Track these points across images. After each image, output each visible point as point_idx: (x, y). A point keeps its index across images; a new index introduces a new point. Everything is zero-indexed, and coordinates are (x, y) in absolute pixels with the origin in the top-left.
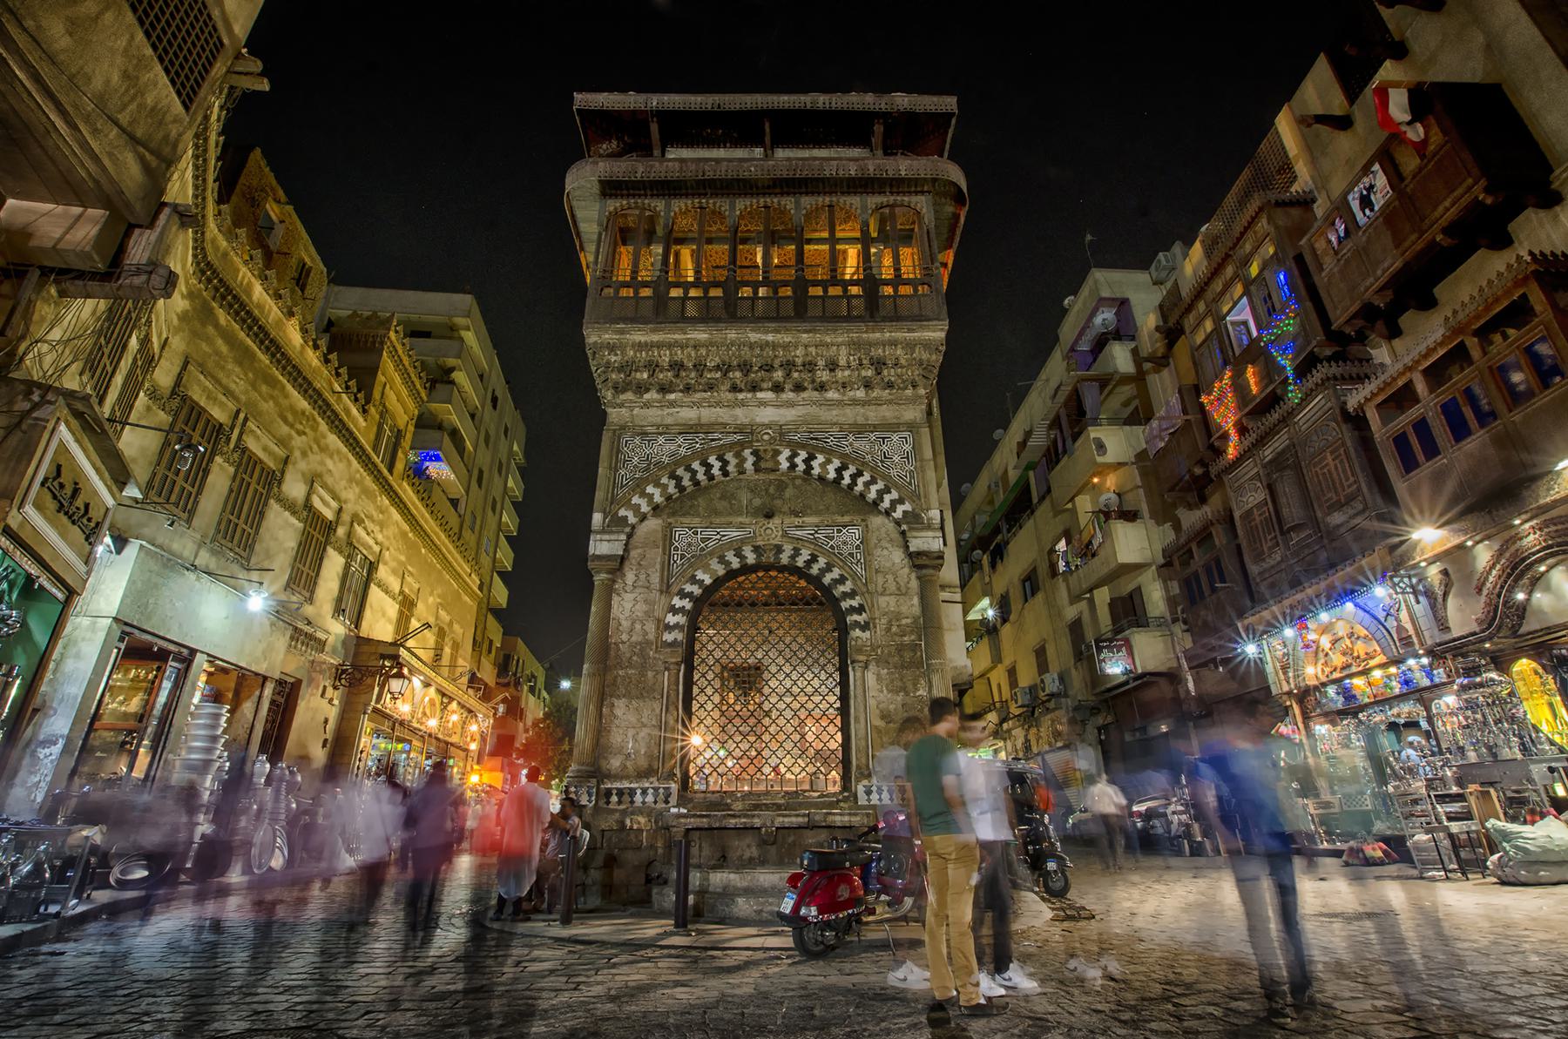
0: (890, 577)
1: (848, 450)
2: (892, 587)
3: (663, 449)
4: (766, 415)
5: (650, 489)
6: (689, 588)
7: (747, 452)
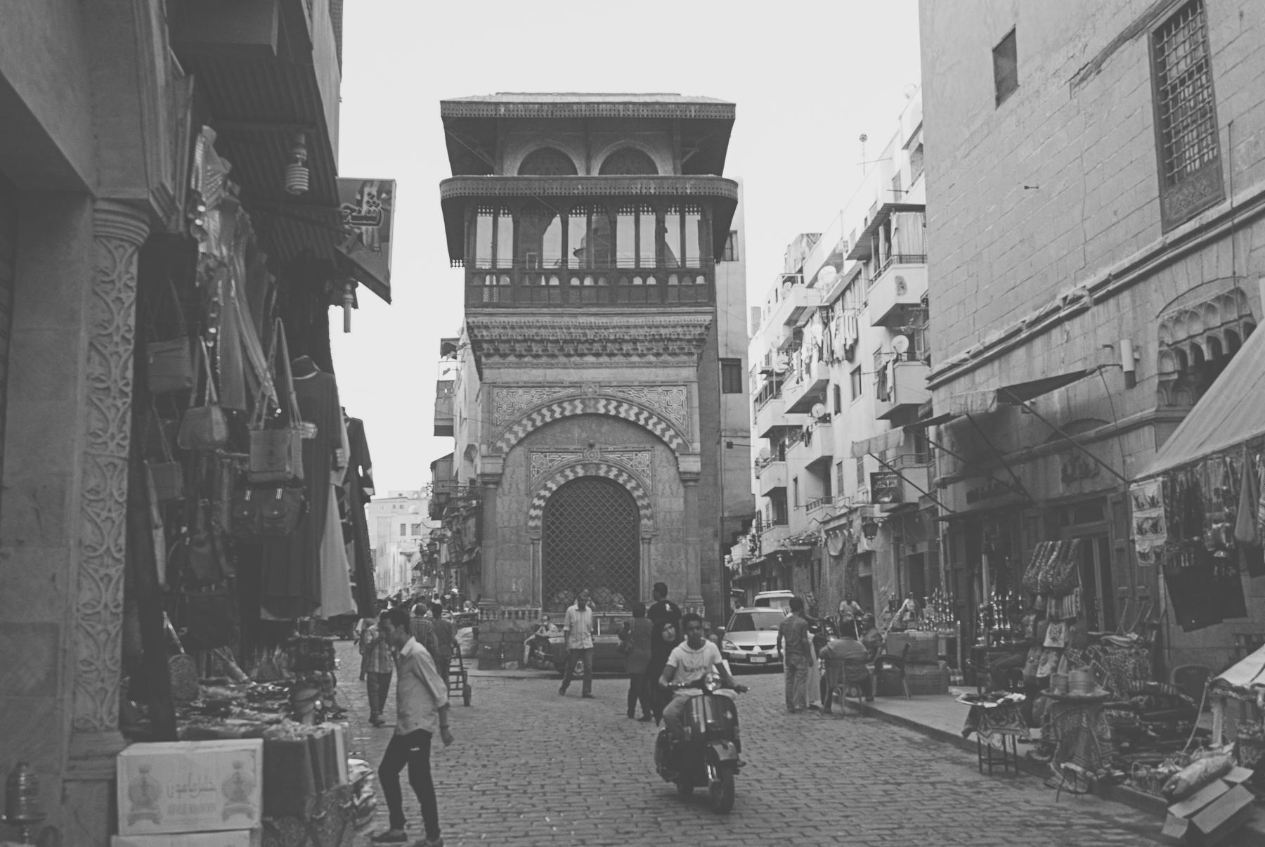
0: (667, 486)
1: (643, 400)
2: (668, 491)
3: (523, 399)
4: (589, 375)
5: (516, 428)
6: (543, 493)
7: (577, 402)
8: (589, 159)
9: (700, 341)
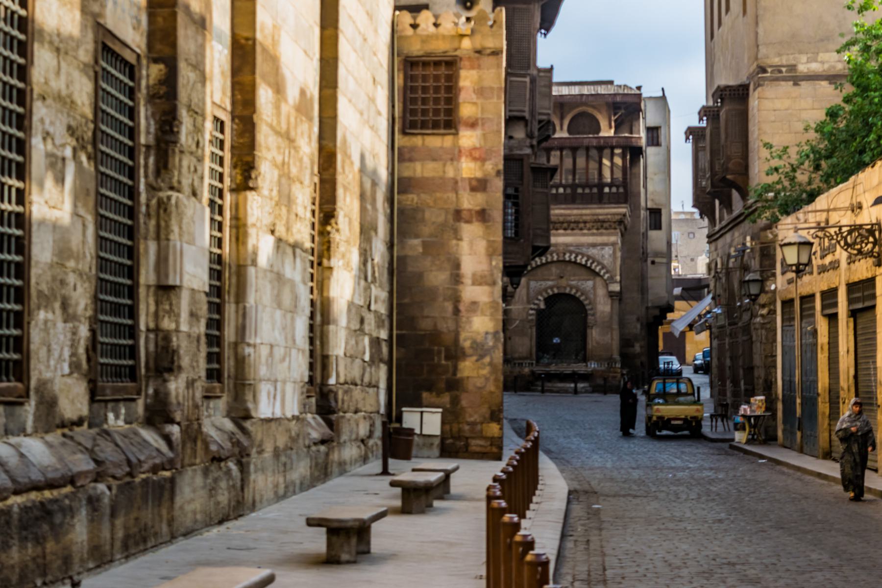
1: (590, 253)
2: (602, 301)
8: (562, 119)
9: (621, 222)
